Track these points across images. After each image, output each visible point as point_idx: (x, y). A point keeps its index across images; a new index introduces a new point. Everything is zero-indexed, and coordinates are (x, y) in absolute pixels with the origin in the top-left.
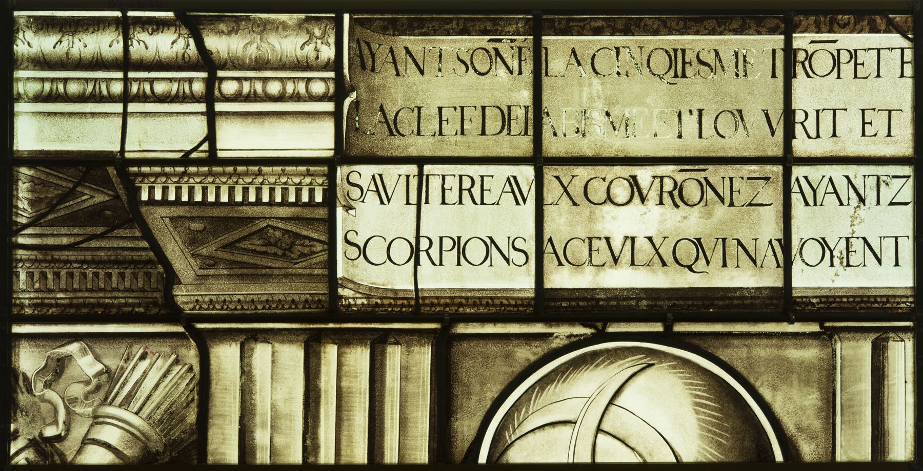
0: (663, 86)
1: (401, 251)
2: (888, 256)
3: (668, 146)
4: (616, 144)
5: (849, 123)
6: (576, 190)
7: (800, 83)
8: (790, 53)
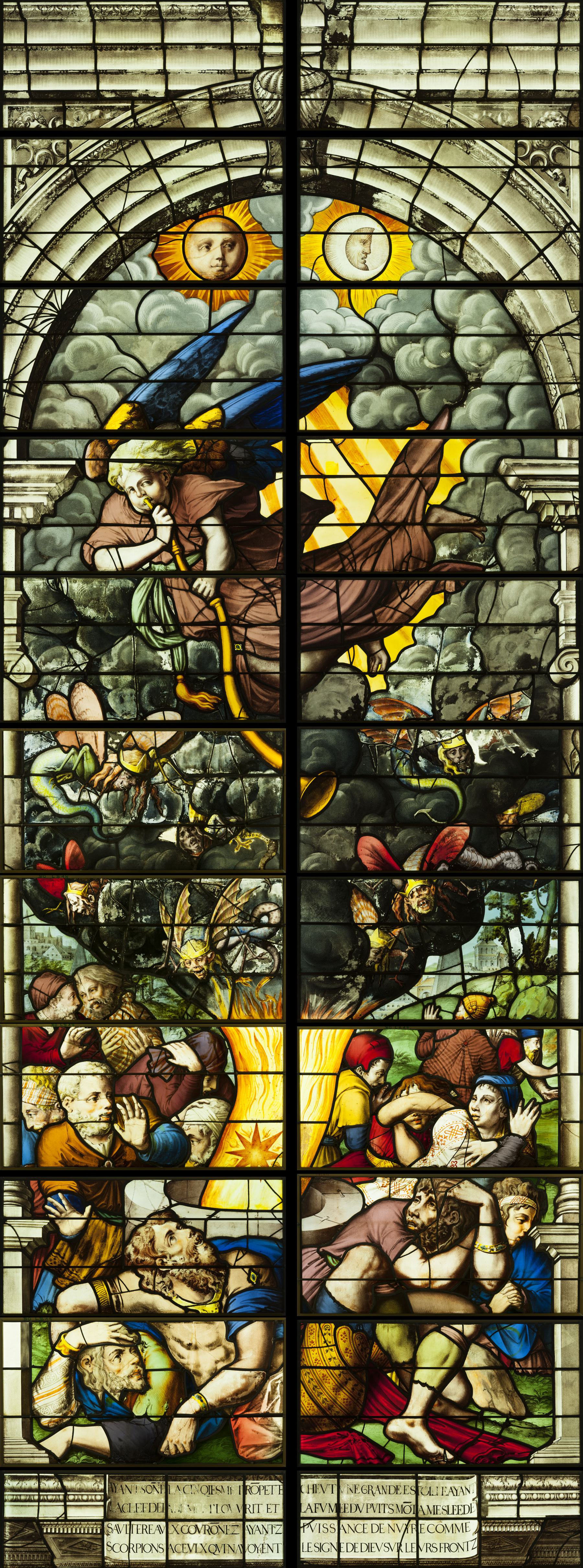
0: (205, 1497)
1: (124, 1548)
2: (275, 1550)
3: (207, 1515)
4: (191, 1515)
5: (263, 1508)
6: (179, 1529)
7: (248, 1496)
8: (245, 1487)
